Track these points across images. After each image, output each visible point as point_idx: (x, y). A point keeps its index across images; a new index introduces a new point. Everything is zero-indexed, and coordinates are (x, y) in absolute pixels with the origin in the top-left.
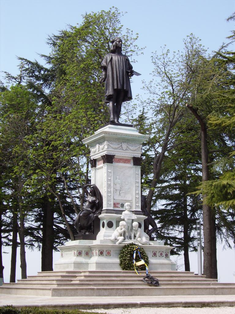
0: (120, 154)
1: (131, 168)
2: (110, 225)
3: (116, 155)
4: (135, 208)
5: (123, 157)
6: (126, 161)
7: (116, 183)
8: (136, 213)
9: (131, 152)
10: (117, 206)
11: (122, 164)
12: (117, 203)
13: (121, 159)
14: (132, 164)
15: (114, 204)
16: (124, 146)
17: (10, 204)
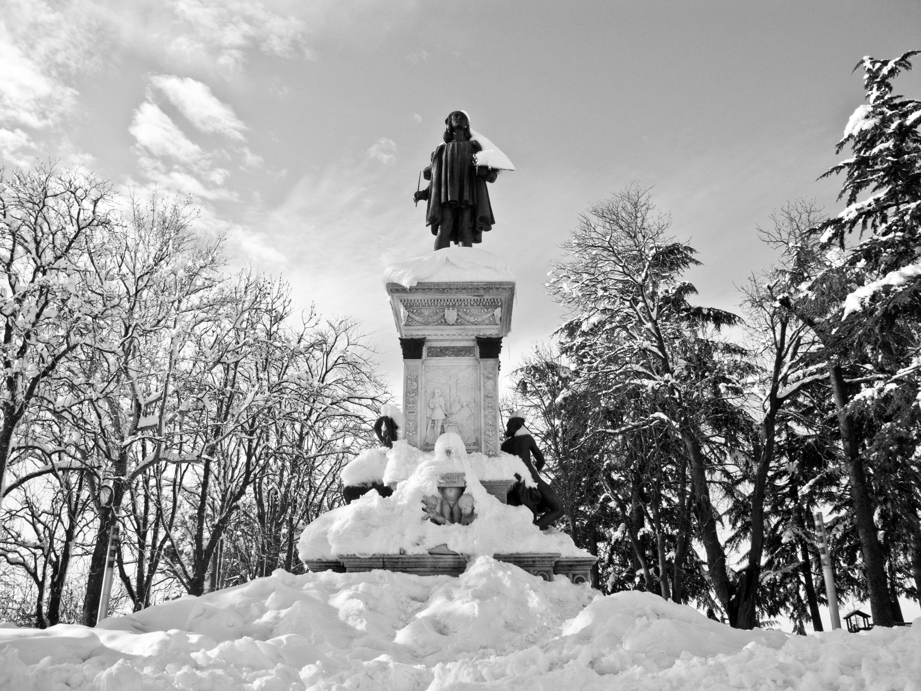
3: (428, 338)
5: (452, 340)
6: (458, 352)
7: (432, 406)
9: (474, 327)
13: (447, 349)
14: (478, 356)
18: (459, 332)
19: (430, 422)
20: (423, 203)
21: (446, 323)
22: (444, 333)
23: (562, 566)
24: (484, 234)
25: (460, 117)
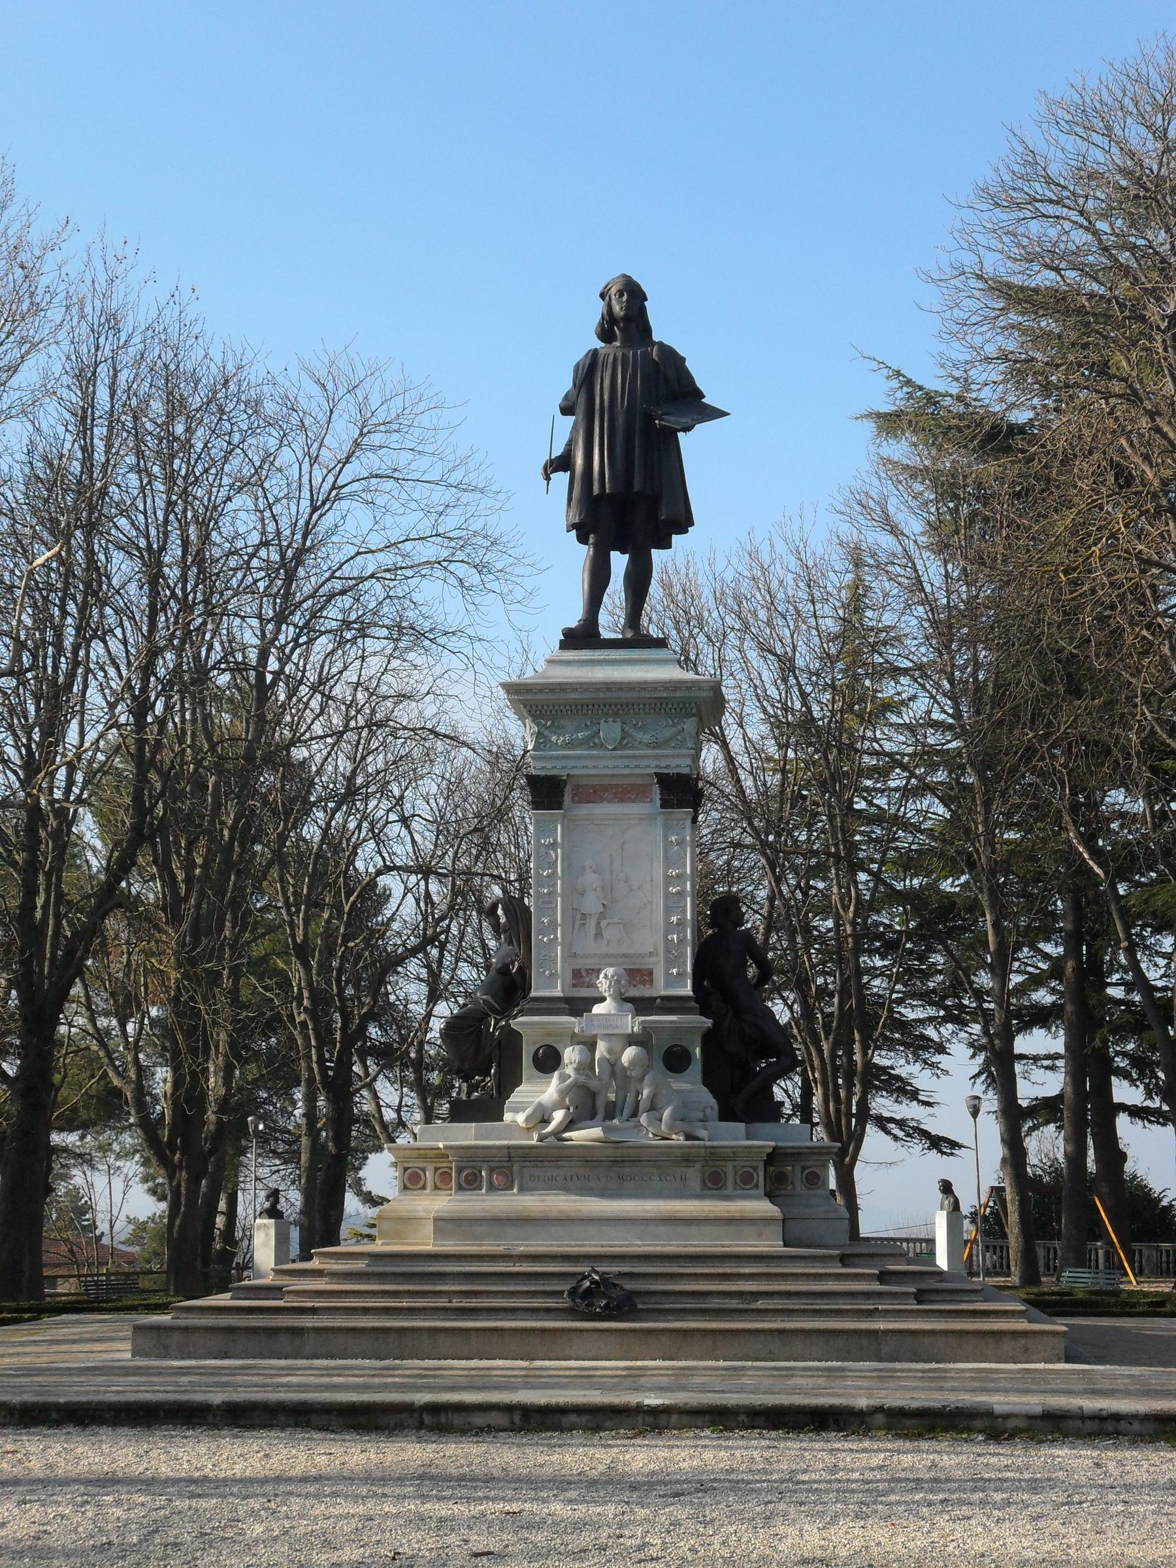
0: (607, 767)
1: (652, 818)
2: (548, 1061)
4: (667, 985)
6: (626, 792)
8: (671, 1004)
10: (587, 979)
11: (610, 805)
12: (587, 971)
13: (605, 788)
14: (658, 803)
15: (577, 974)
16: (610, 730)
17: (873, 972)
18: (626, 762)
19: (578, 917)
20: (561, 479)
21: (601, 746)
22: (601, 763)
23: (786, 1154)
24: (676, 539)
25: (633, 293)
